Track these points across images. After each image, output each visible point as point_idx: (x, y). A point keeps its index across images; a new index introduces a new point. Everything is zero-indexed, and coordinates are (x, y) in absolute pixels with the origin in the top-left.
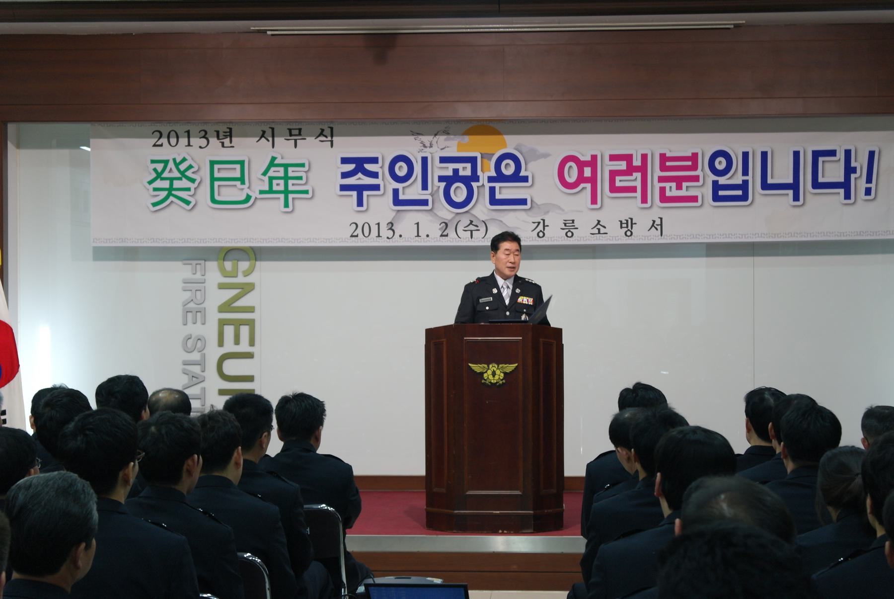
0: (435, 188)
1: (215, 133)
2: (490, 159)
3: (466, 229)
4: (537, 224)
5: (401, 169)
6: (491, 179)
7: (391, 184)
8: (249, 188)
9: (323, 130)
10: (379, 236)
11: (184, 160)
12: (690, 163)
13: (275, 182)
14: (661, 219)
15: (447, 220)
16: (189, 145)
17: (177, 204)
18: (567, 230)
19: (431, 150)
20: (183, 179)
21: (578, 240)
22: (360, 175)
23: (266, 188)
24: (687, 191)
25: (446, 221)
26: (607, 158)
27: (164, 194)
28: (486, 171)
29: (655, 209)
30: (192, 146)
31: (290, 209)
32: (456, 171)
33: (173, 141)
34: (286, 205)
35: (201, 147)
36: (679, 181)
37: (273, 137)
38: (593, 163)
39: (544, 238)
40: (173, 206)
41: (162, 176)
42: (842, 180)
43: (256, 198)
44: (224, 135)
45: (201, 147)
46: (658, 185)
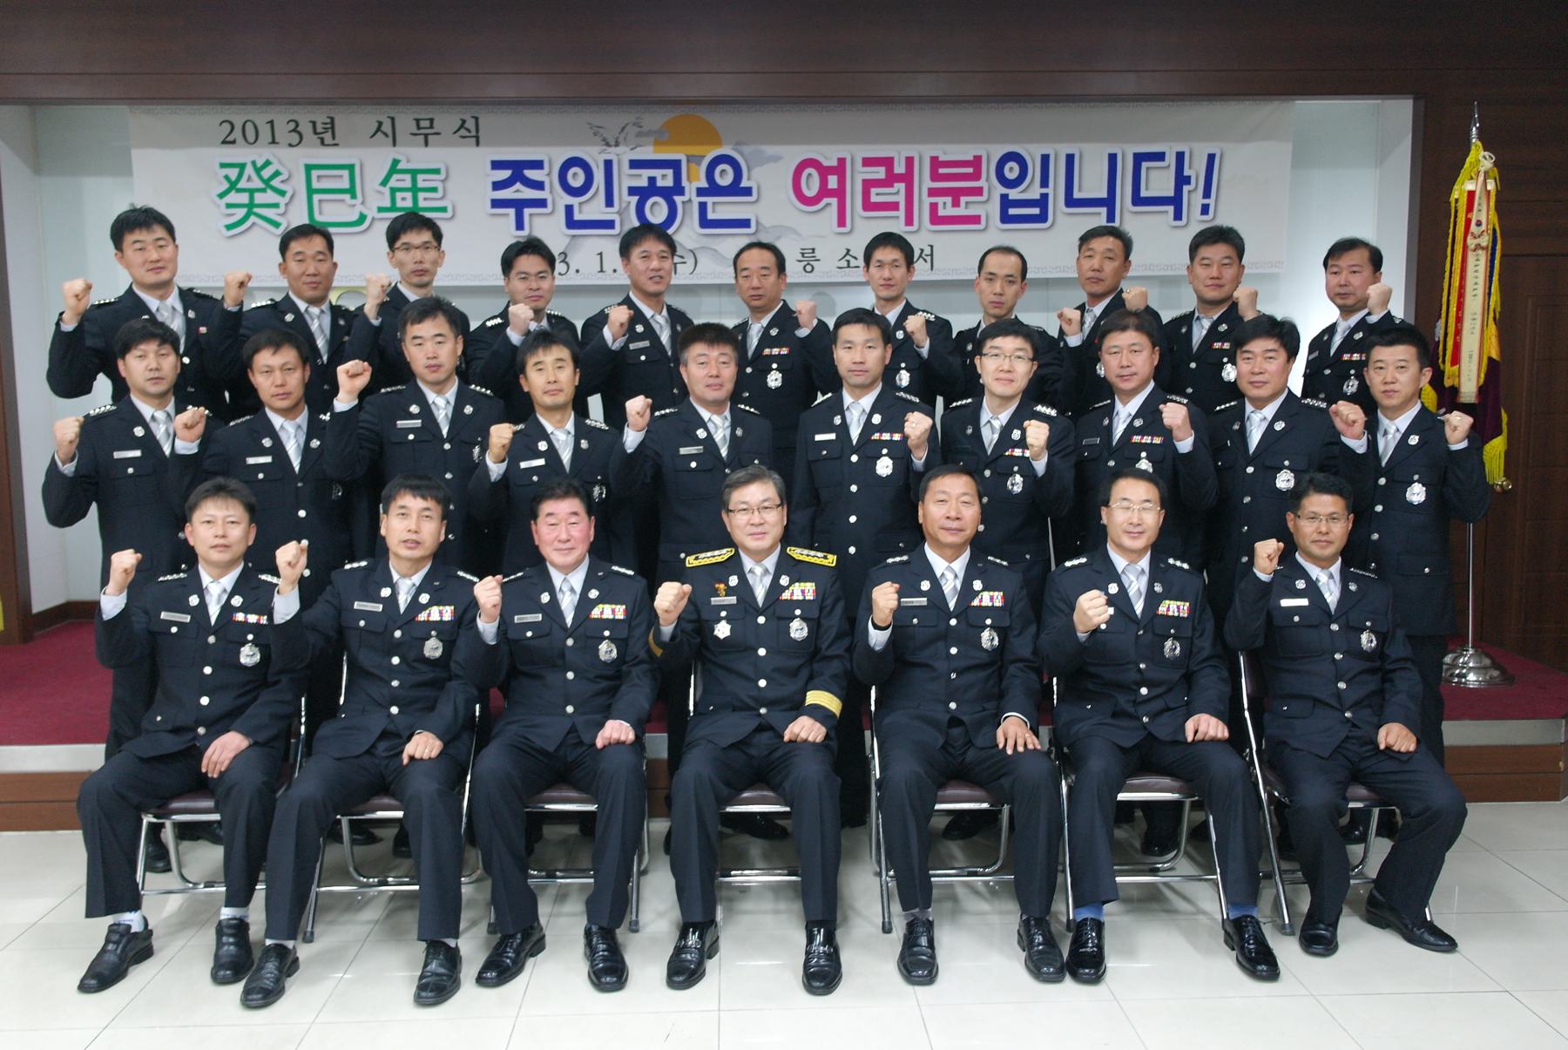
0: (624, 205)
1: (311, 125)
2: (699, 164)
5: (576, 178)
6: (700, 192)
7: (562, 198)
8: (363, 203)
9: (464, 122)
11: (268, 163)
12: (970, 170)
13: (399, 195)
14: (932, 247)
17: (262, 228)
18: (806, 263)
20: (268, 190)
21: (820, 276)
22: (518, 186)
23: (387, 204)
24: (966, 208)
26: (859, 162)
27: (241, 212)
28: (695, 181)
29: (923, 233)
30: (278, 143)
32: (652, 180)
35: (290, 145)
36: (956, 195)
38: (840, 169)
40: (255, 229)
41: (239, 186)
42: (1171, 193)
43: (373, 219)
46: (927, 201)
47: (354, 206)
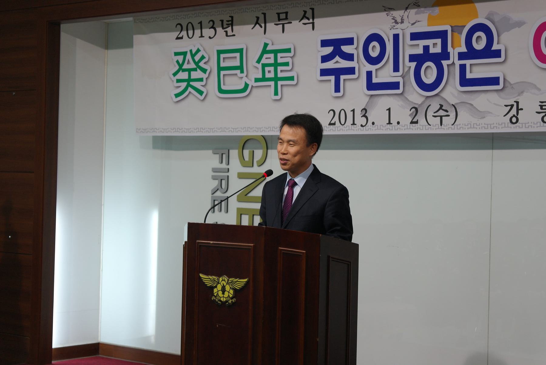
0: (406, 69)
2: (461, 33)
3: (435, 114)
4: (509, 107)
6: (462, 56)
8: (246, 76)
9: (305, 12)
10: (354, 124)
11: (198, 51)
13: (267, 69)
15: (417, 104)
16: (202, 36)
17: (193, 94)
18: (544, 114)
19: (403, 26)
22: (337, 58)
23: (260, 76)
25: (416, 106)
27: (184, 85)
30: (204, 37)
31: (278, 97)
32: (426, 48)
33: (190, 33)
34: (276, 93)
35: (210, 38)
37: (265, 23)
39: (517, 124)
40: (191, 96)
41: (183, 68)
44: (227, 24)
45: (210, 38)
47: (242, 78)
